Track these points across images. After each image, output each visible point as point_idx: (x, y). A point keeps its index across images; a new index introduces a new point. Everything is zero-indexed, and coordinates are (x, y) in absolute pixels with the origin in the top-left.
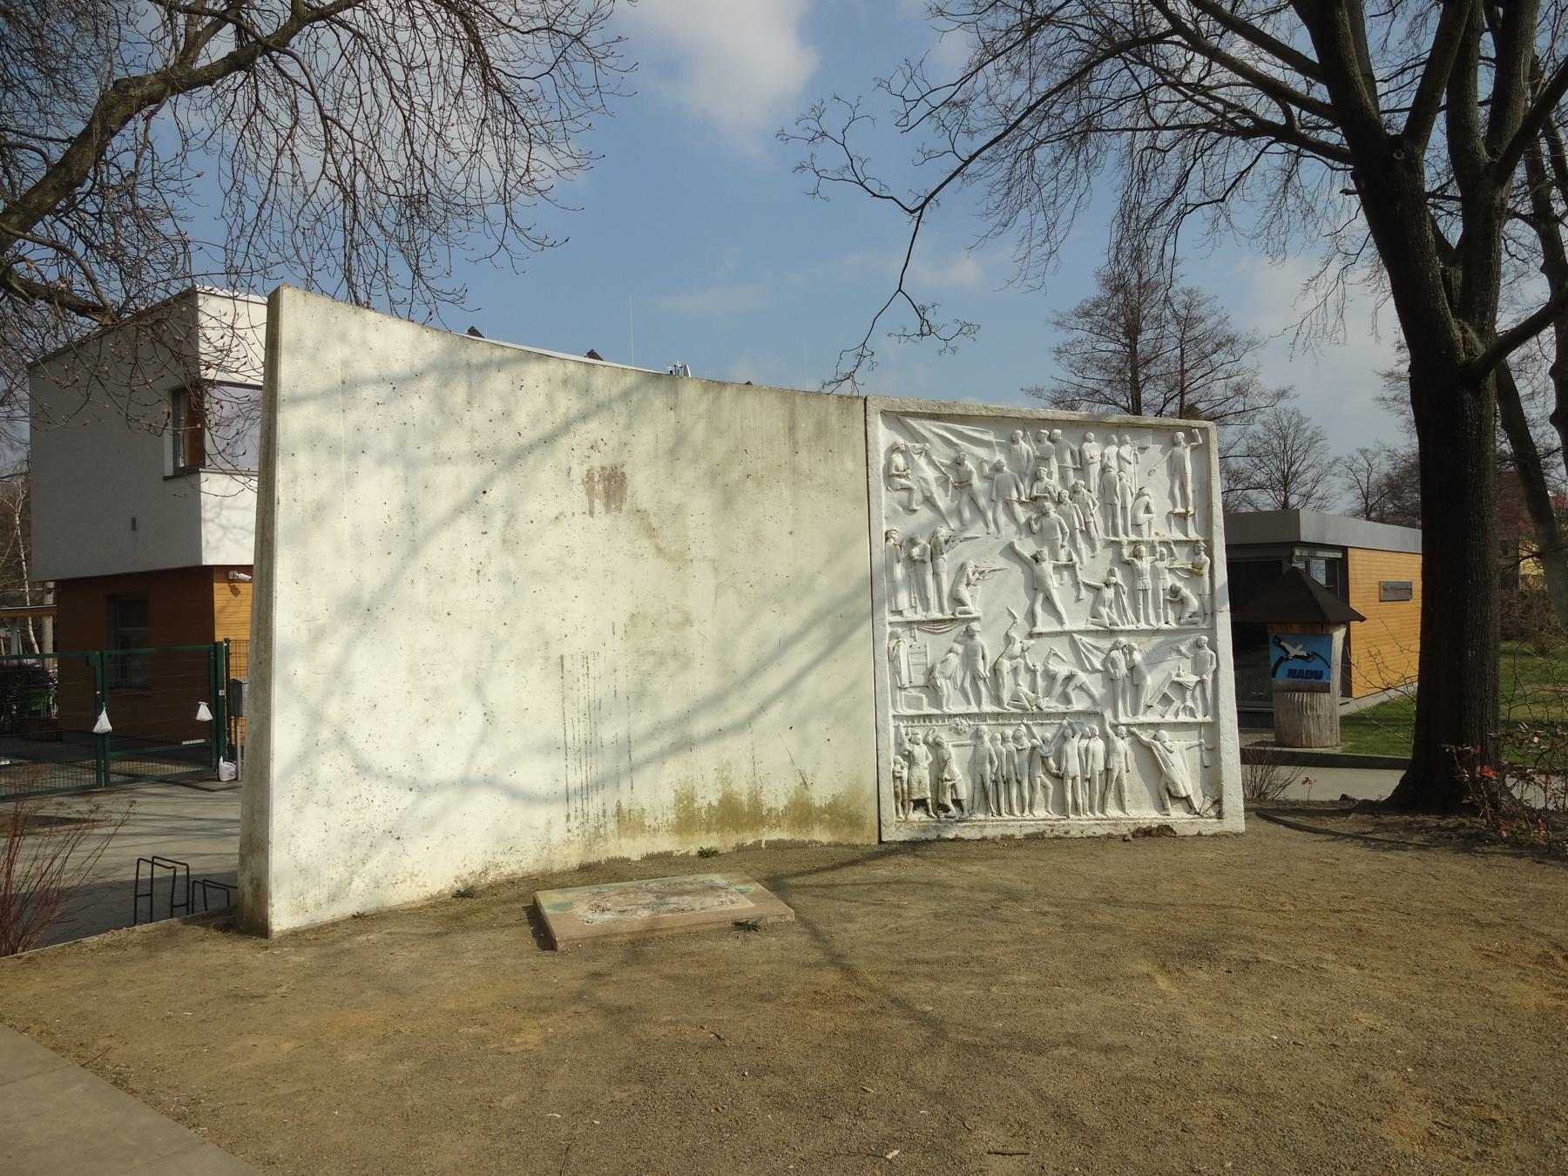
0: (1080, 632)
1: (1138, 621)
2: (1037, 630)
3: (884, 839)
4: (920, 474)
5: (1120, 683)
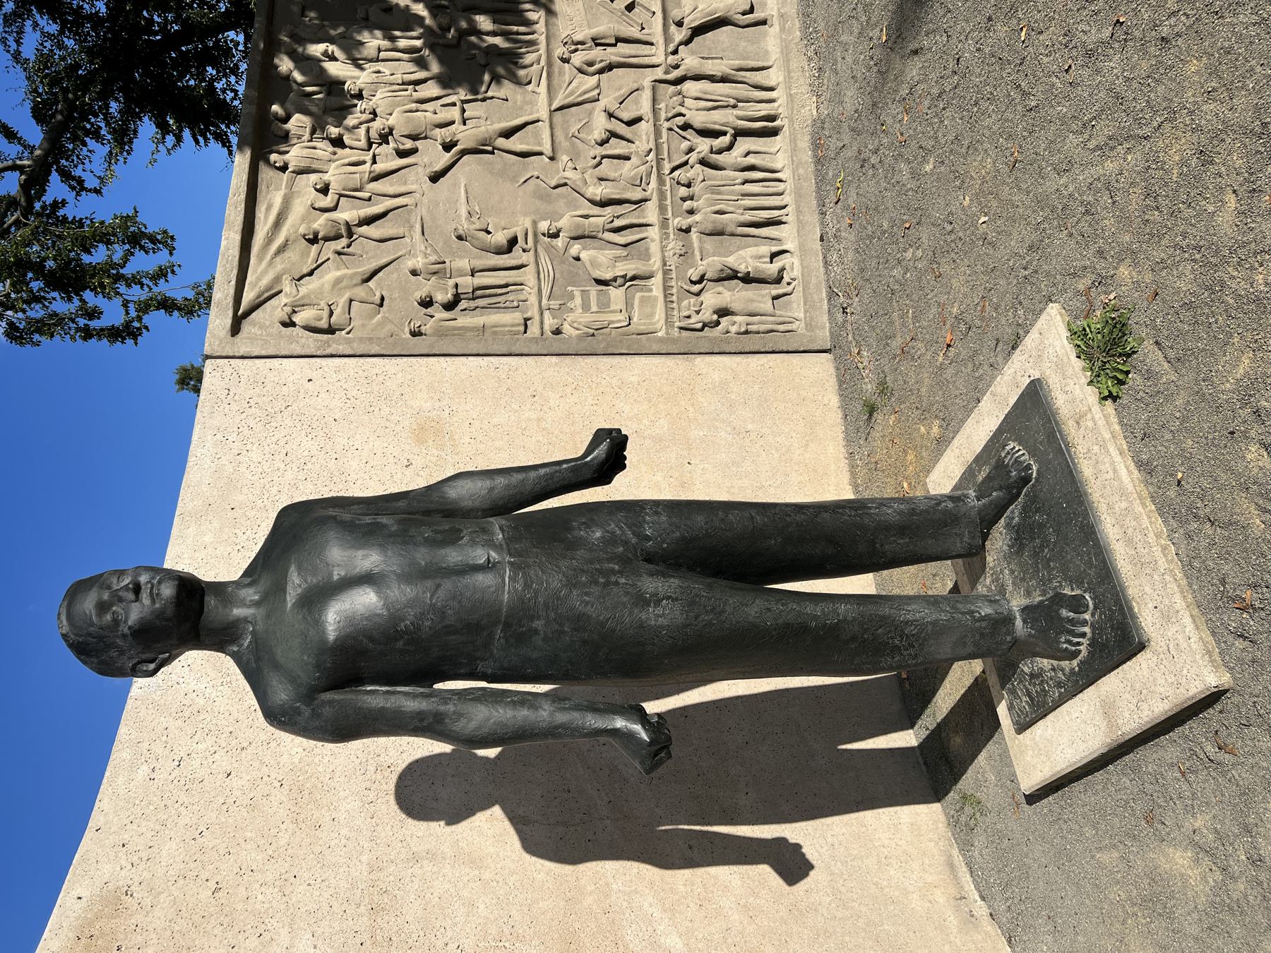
0: (550, 105)
2: (547, 148)
4: (327, 287)
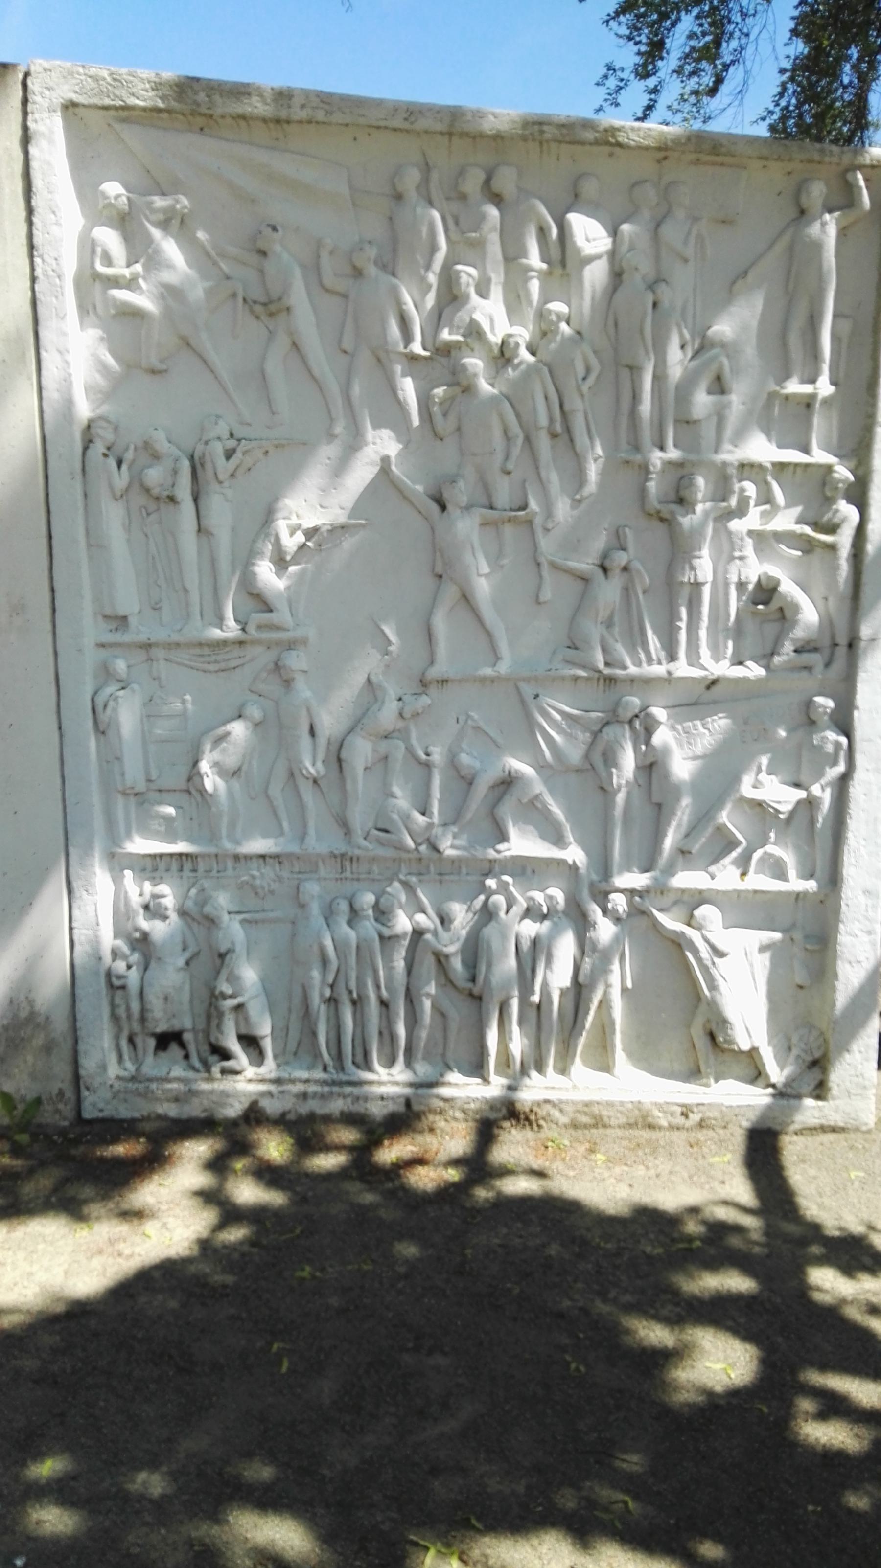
1: (672, 657)
3: (87, 1114)
5: (620, 798)
